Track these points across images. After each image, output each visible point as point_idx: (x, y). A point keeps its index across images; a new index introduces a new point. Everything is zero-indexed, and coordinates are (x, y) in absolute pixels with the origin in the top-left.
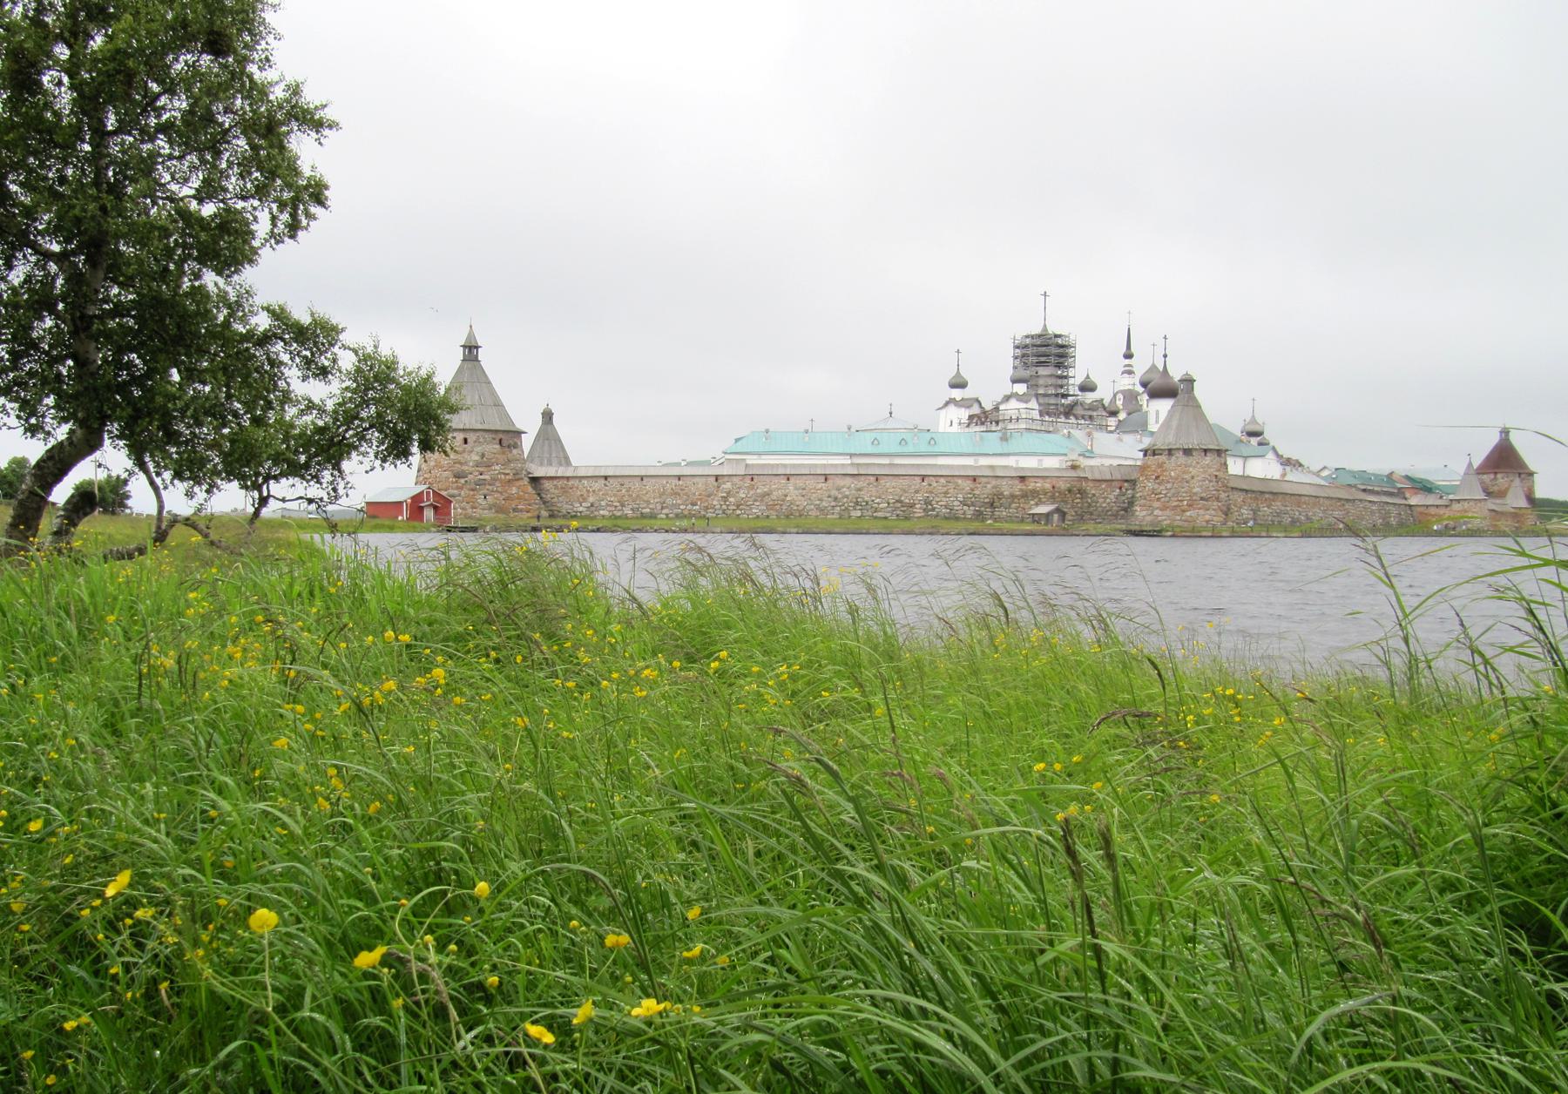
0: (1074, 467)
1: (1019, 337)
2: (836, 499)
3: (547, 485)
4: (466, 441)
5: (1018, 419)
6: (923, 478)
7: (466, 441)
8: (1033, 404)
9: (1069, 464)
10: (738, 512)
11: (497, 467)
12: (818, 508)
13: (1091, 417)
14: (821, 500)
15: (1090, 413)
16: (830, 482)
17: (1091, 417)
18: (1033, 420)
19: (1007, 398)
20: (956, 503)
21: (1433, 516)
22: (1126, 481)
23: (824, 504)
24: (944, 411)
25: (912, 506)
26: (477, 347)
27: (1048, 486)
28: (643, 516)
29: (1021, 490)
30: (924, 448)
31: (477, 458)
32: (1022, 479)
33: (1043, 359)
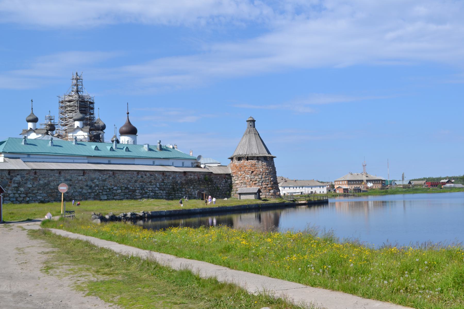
2: (91, 187)
20: (157, 189)
23: (84, 191)
25: (134, 191)
27: (196, 177)
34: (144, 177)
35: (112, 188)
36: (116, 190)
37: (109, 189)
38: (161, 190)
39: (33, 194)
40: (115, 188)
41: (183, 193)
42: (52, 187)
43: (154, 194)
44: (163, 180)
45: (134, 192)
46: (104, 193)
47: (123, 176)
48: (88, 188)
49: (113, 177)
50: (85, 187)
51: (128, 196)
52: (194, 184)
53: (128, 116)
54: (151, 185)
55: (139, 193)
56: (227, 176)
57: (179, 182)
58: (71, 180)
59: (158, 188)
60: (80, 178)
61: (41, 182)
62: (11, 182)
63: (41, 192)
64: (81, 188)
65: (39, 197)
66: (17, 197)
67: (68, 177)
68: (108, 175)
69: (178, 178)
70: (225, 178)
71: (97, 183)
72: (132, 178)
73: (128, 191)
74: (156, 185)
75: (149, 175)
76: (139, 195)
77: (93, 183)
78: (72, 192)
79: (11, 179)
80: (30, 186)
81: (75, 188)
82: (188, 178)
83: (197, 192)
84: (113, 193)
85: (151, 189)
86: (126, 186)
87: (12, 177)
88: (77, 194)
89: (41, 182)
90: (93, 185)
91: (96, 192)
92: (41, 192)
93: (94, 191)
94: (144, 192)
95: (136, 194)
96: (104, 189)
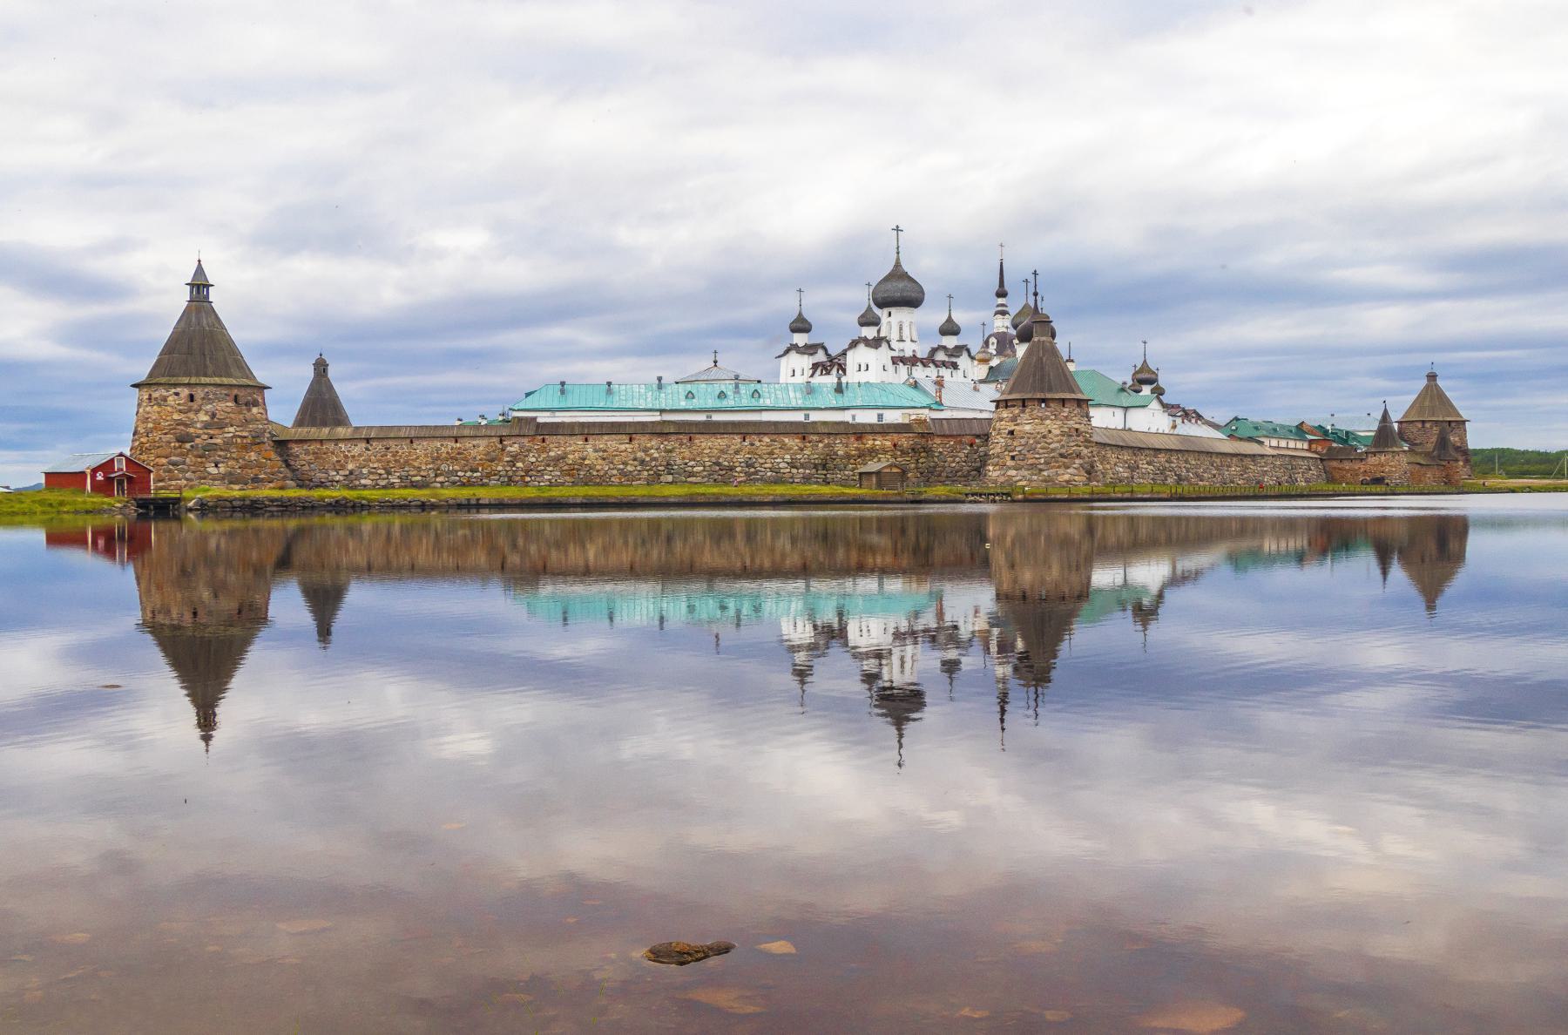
2: (642, 462)
3: (296, 449)
4: (192, 398)
7: (192, 398)
10: (528, 479)
11: (231, 429)
12: (623, 473)
16: (635, 442)
19: (854, 344)
21: (1348, 471)
22: (978, 436)
23: (630, 468)
24: (784, 360)
25: (732, 469)
26: (208, 286)
27: (888, 443)
29: (857, 449)
30: (746, 401)
34: (758, 444)
35: (686, 464)
38: (793, 467)
39: (539, 471)
40: (692, 463)
41: (847, 473)
42: (571, 462)
45: (731, 470)
47: (709, 444)
48: (636, 463)
50: (631, 462)
51: (716, 477)
52: (880, 456)
53: (1036, 300)
56: (977, 441)
57: (839, 453)
58: (605, 451)
59: (788, 463)
60: (623, 447)
61: (552, 454)
63: (551, 469)
67: (601, 446)
70: (971, 445)
71: (656, 455)
72: (730, 446)
73: (718, 468)
74: (783, 459)
75: (769, 440)
79: (503, 450)
80: (534, 460)
81: (612, 463)
82: (867, 446)
84: (685, 471)
86: (714, 460)
87: (506, 446)
88: (615, 472)
89: (552, 454)
92: (551, 469)
94: (752, 470)
95: (736, 474)
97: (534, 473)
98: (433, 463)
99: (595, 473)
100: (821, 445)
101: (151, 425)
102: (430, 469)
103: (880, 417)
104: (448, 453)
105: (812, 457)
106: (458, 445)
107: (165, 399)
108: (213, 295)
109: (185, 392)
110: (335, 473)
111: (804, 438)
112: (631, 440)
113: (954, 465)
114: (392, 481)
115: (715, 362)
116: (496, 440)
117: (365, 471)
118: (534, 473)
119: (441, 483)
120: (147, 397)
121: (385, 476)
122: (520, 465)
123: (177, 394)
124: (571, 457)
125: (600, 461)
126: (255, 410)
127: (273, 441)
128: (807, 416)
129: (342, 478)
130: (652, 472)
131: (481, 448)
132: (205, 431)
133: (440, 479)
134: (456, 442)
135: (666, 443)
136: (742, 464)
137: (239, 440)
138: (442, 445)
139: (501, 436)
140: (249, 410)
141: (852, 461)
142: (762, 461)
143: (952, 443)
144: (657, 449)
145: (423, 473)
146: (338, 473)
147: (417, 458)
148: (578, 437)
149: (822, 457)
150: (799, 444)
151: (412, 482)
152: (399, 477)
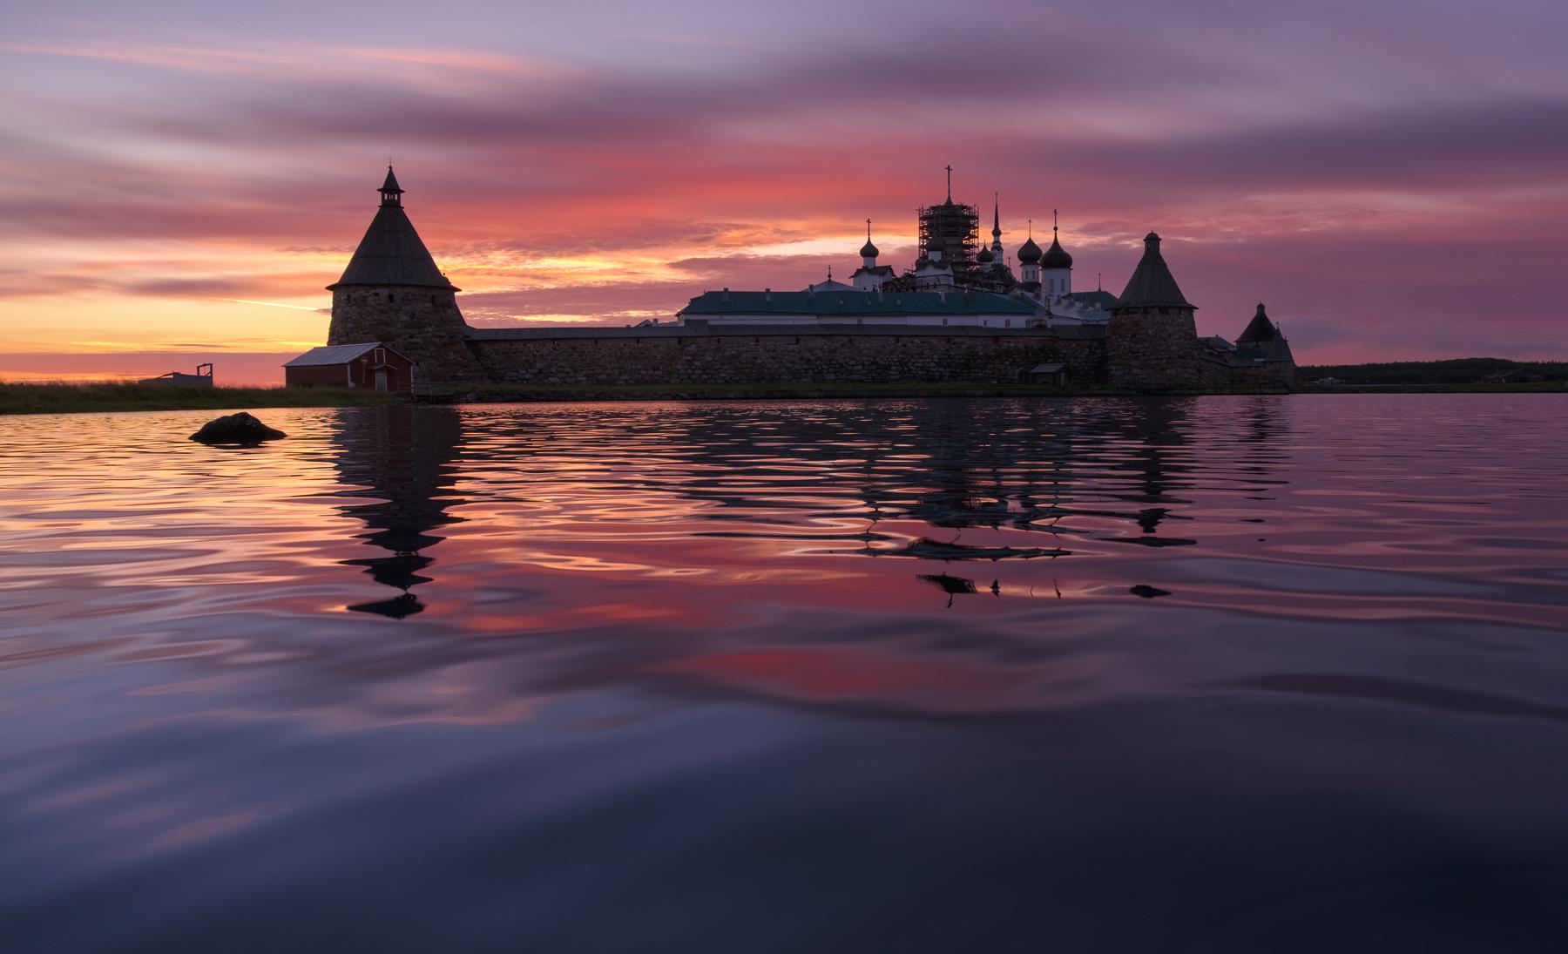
0: (1041, 327)
1: (927, 207)
2: (808, 361)
3: (487, 349)
5: (935, 286)
6: (898, 338)
7: (391, 298)
8: (949, 271)
9: (1036, 323)
11: (430, 329)
13: (992, 286)
14: (793, 362)
15: (990, 281)
17: (992, 286)
18: (949, 285)
26: (400, 192)
27: (1021, 346)
28: (599, 382)
31: (405, 318)
32: (996, 338)
33: (951, 229)
34: (910, 345)
35: (847, 363)
36: (853, 366)
37: (841, 365)
40: (853, 362)
42: (744, 361)
43: (925, 373)
44: (947, 350)
46: (831, 370)
47: (868, 345)
48: (803, 362)
49: (849, 345)
51: (874, 375)
54: (921, 358)
55: (896, 370)
56: (1095, 344)
57: (981, 353)
58: (774, 351)
60: (791, 347)
61: (727, 354)
62: (681, 354)
63: (726, 367)
64: (791, 362)
65: (722, 375)
66: (690, 375)
68: (841, 342)
69: (980, 347)
71: (820, 355)
73: (874, 367)
76: (895, 375)
77: (813, 355)
78: (777, 366)
79: (682, 350)
80: (710, 359)
83: (1017, 371)
85: (920, 365)
86: (872, 359)
88: (784, 370)
90: (813, 358)
91: (817, 368)
92: (726, 367)
93: (814, 366)
94: (906, 369)
96: (831, 364)
97: (711, 372)
98: (618, 361)
99: (766, 371)
100: (964, 346)
101: (350, 325)
102: (615, 368)
103: (1008, 322)
104: (631, 352)
105: (957, 357)
106: (640, 345)
107: (365, 299)
108: (405, 202)
109: (384, 292)
110: (524, 372)
111: (949, 340)
112: (797, 342)
113: (1076, 365)
114: (579, 379)
115: (830, 276)
116: (675, 341)
117: (553, 370)
118: (711, 372)
119: (625, 381)
120: (346, 297)
121: (572, 374)
122: (697, 363)
123: (377, 294)
124: (745, 356)
125: (771, 361)
126: (449, 312)
127: (466, 342)
128: (945, 321)
129: (531, 377)
130: (817, 371)
131: (661, 348)
132: (406, 331)
133: (622, 378)
134: (638, 342)
135: (828, 343)
136: (898, 364)
137: (437, 340)
138: (625, 345)
139: (679, 337)
140: (445, 312)
141: (991, 361)
142: (912, 360)
143: (1074, 346)
144: (821, 350)
145: (607, 372)
146: (527, 372)
147: (602, 357)
148: (751, 338)
149: (966, 357)
150: (946, 346)
151: (598, 380)
152: (585, 376)
